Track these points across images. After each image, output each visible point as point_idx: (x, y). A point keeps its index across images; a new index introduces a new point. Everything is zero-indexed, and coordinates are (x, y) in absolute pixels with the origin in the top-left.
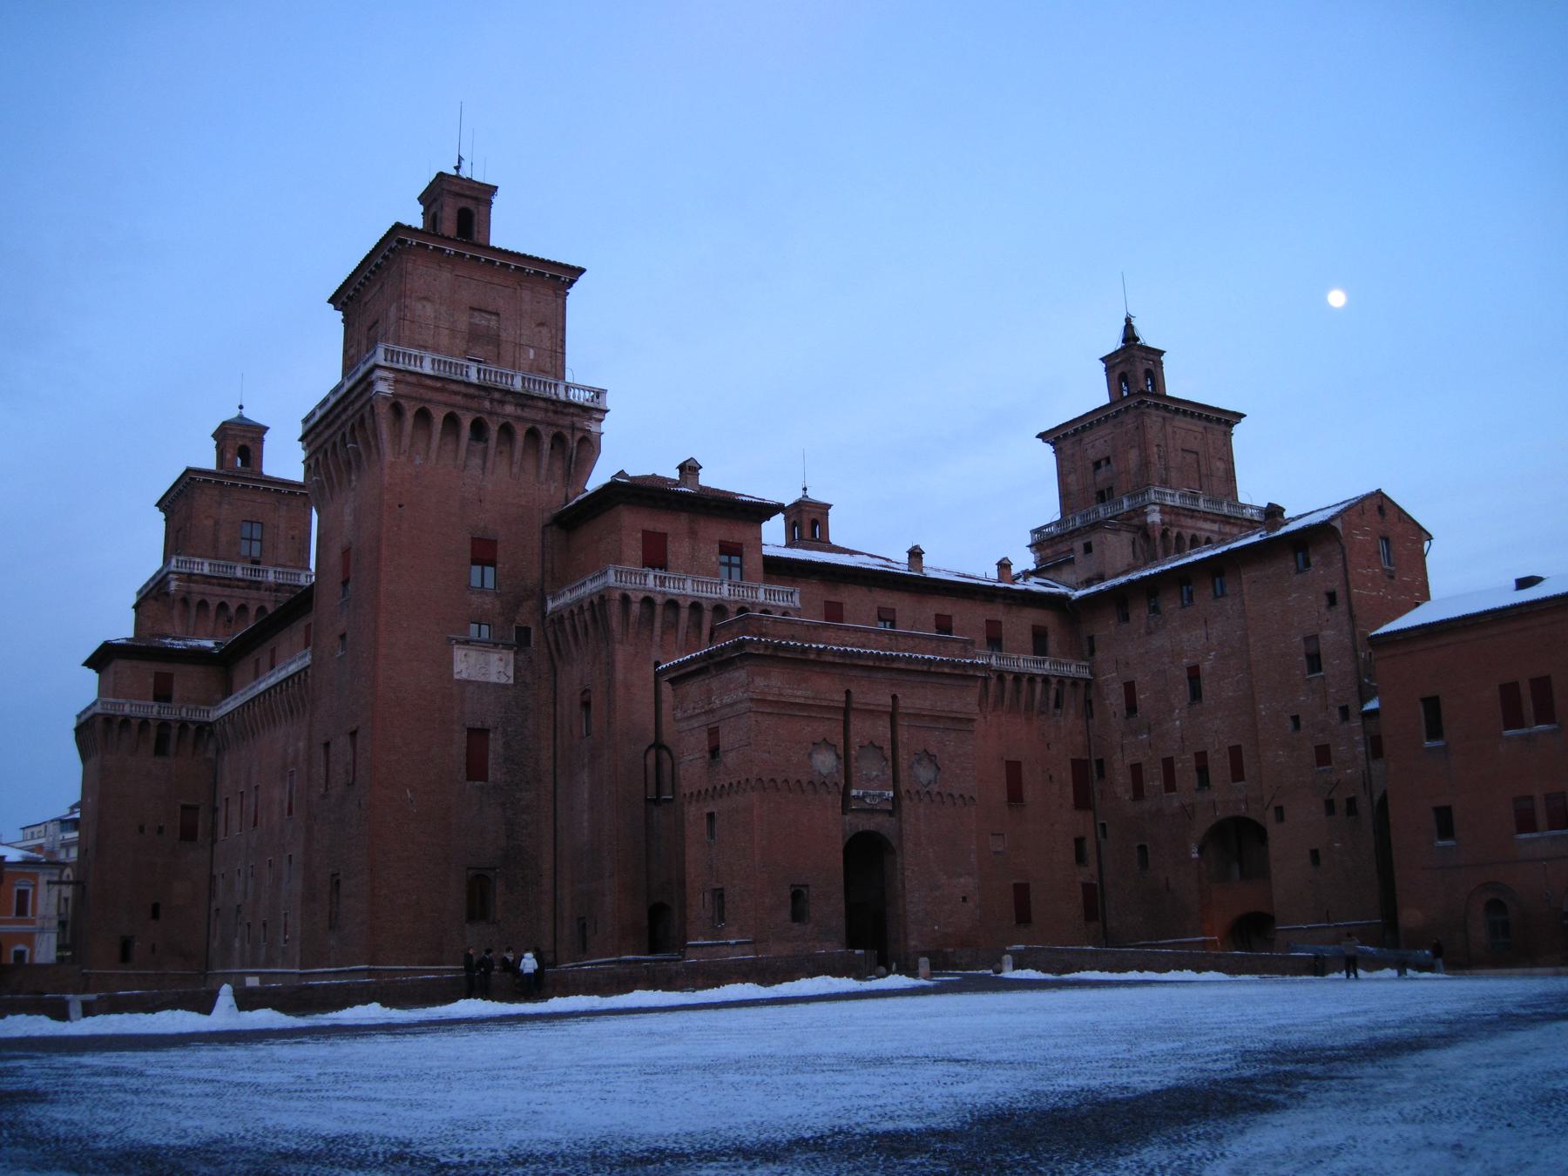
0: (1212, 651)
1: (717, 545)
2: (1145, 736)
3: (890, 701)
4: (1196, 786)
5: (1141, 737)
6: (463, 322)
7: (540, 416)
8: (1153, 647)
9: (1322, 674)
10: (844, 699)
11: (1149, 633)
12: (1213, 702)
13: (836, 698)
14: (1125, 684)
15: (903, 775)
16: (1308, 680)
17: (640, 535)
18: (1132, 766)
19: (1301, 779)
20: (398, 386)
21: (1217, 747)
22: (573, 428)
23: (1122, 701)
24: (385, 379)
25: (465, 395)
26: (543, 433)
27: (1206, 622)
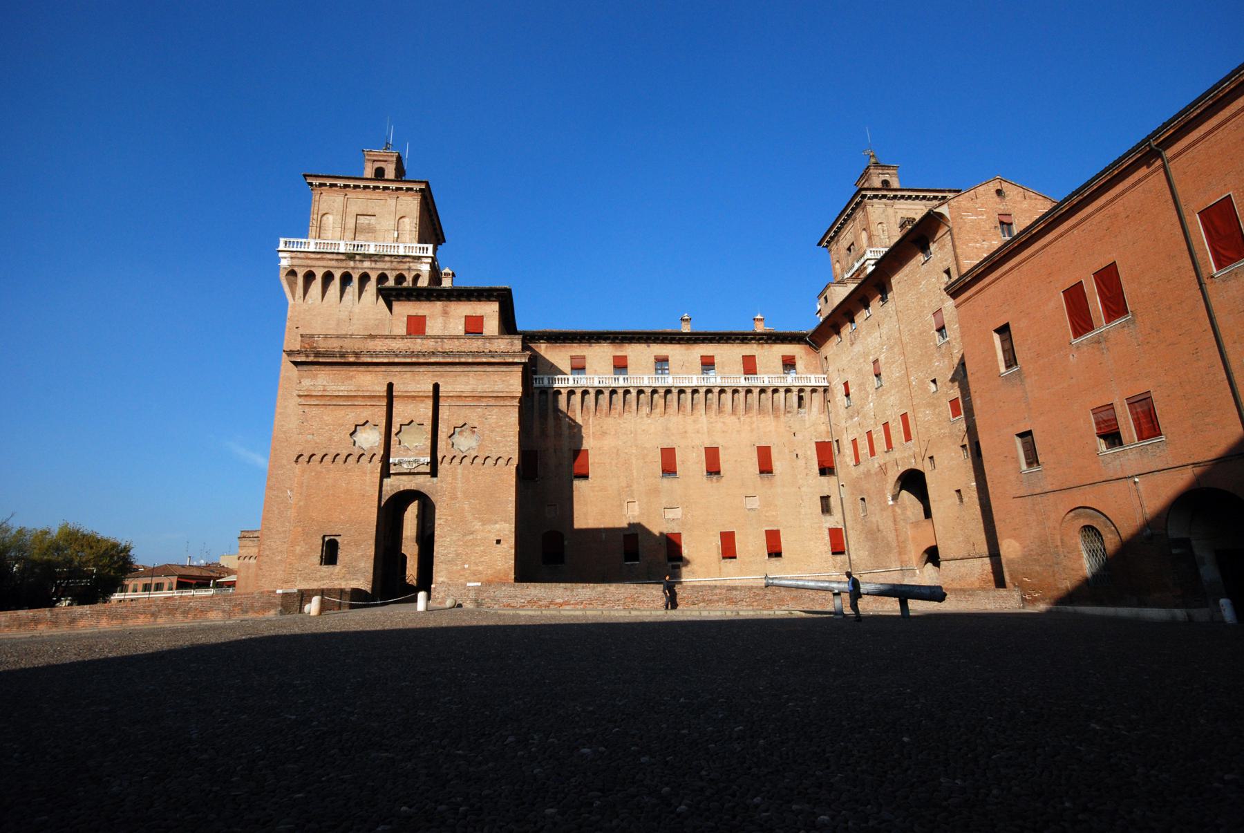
0: (885, 345)
1: (464, 319)
3: (431, 388)
4: (886, 450)
6: (351, 223)
7: (388, 265)
10: (385, 389)
11: (852, 344)
13: (377, 389)
15: (442, 444)
17: (406, 319)
19: (942, 431)
20: (294, 260)
21: (894, 417)
22: (409, 269)
24: (285, 258)
25: (337, 260)
26: (389, 276)
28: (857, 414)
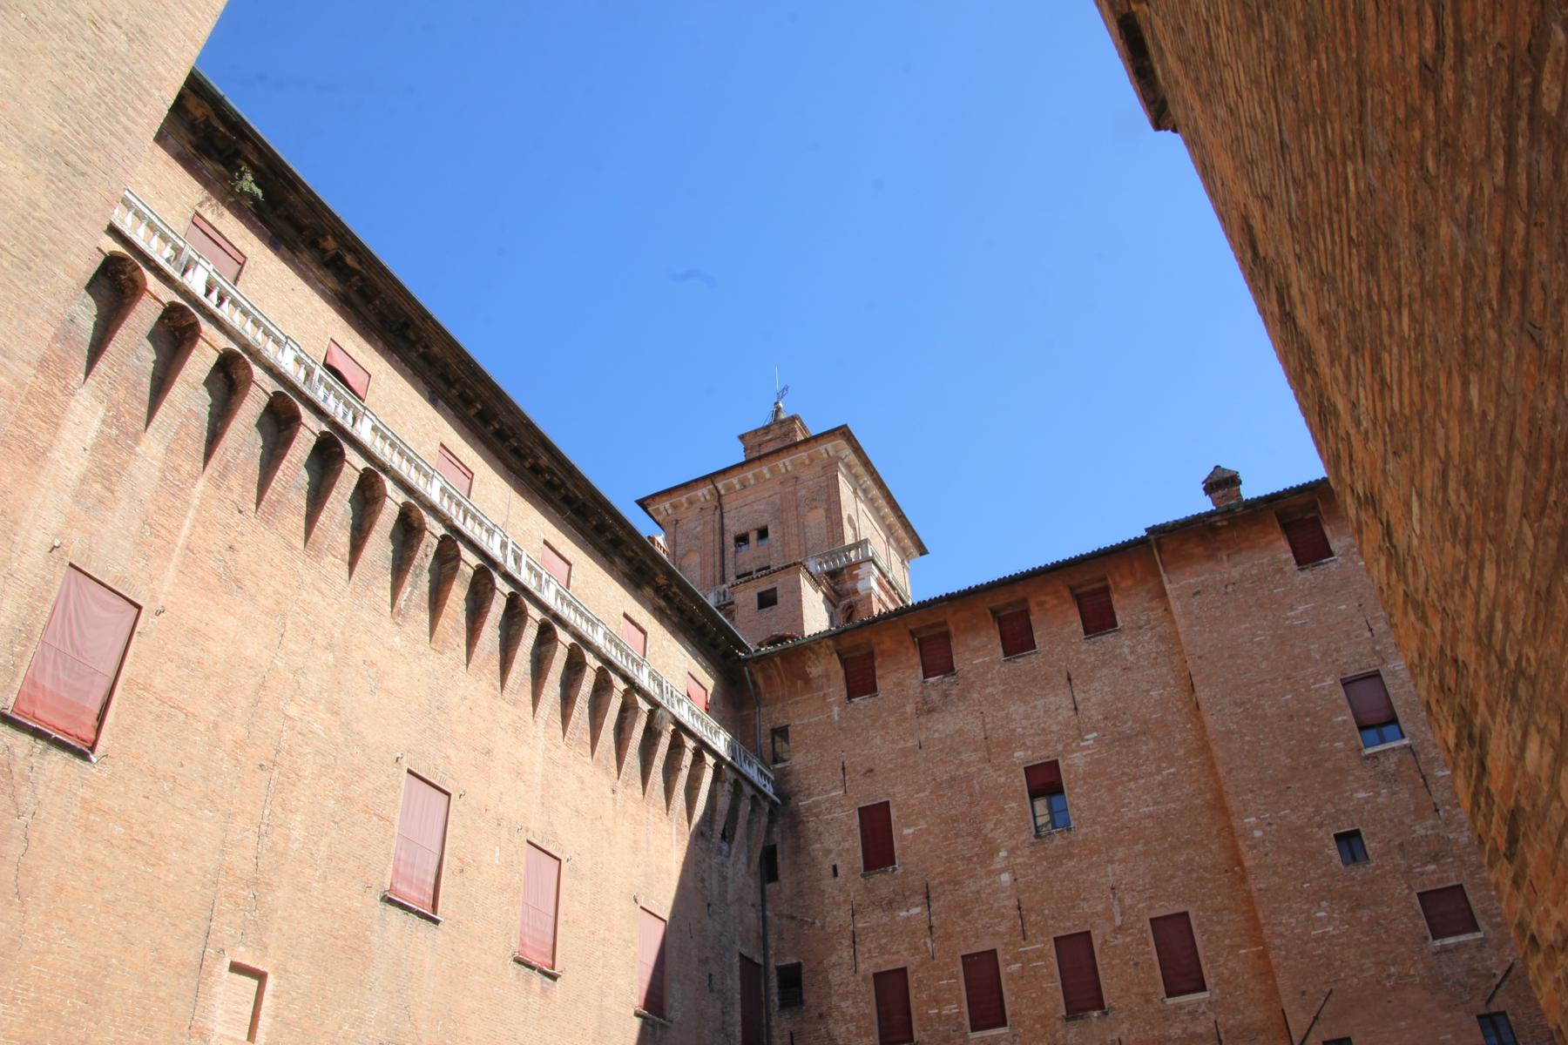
0: (1095, 729)
2: (915, 910)
4: (1064, 1013)
5: (904, 914)
8: (937, 735)
9: (1406, 741)
12: (1099, 828)
14: (860, 810)
16: (1374, 756)
18: (879, 978)
21: (1118, 921)
23: (855, 843)
27: (1069, 679)
28: (918, 899)
